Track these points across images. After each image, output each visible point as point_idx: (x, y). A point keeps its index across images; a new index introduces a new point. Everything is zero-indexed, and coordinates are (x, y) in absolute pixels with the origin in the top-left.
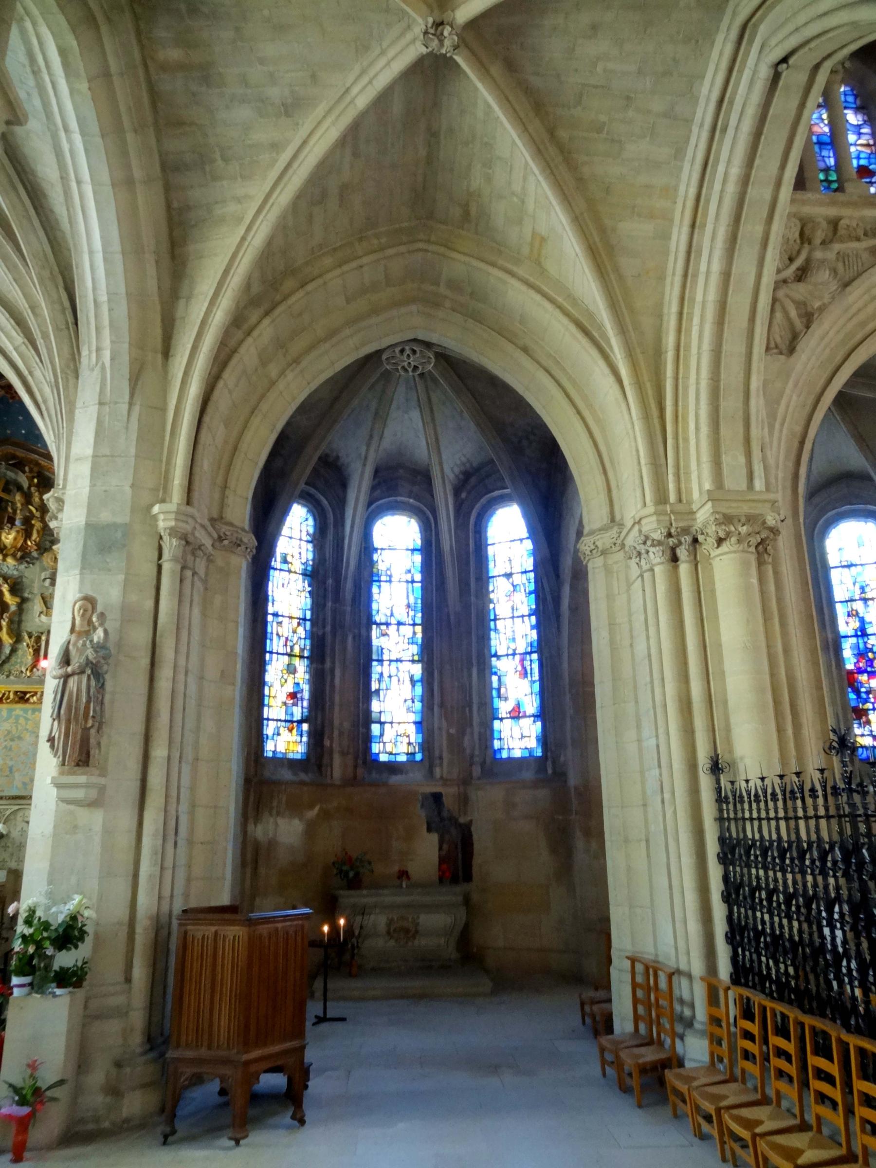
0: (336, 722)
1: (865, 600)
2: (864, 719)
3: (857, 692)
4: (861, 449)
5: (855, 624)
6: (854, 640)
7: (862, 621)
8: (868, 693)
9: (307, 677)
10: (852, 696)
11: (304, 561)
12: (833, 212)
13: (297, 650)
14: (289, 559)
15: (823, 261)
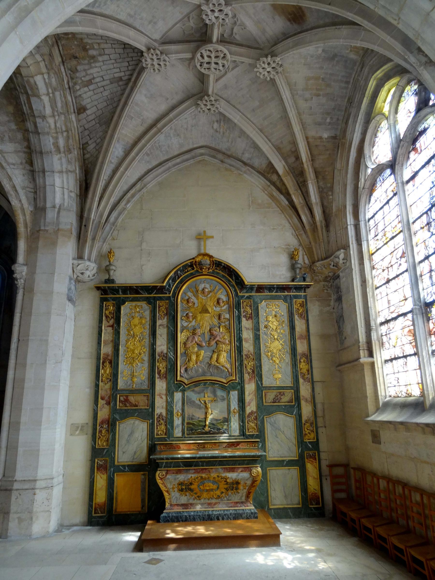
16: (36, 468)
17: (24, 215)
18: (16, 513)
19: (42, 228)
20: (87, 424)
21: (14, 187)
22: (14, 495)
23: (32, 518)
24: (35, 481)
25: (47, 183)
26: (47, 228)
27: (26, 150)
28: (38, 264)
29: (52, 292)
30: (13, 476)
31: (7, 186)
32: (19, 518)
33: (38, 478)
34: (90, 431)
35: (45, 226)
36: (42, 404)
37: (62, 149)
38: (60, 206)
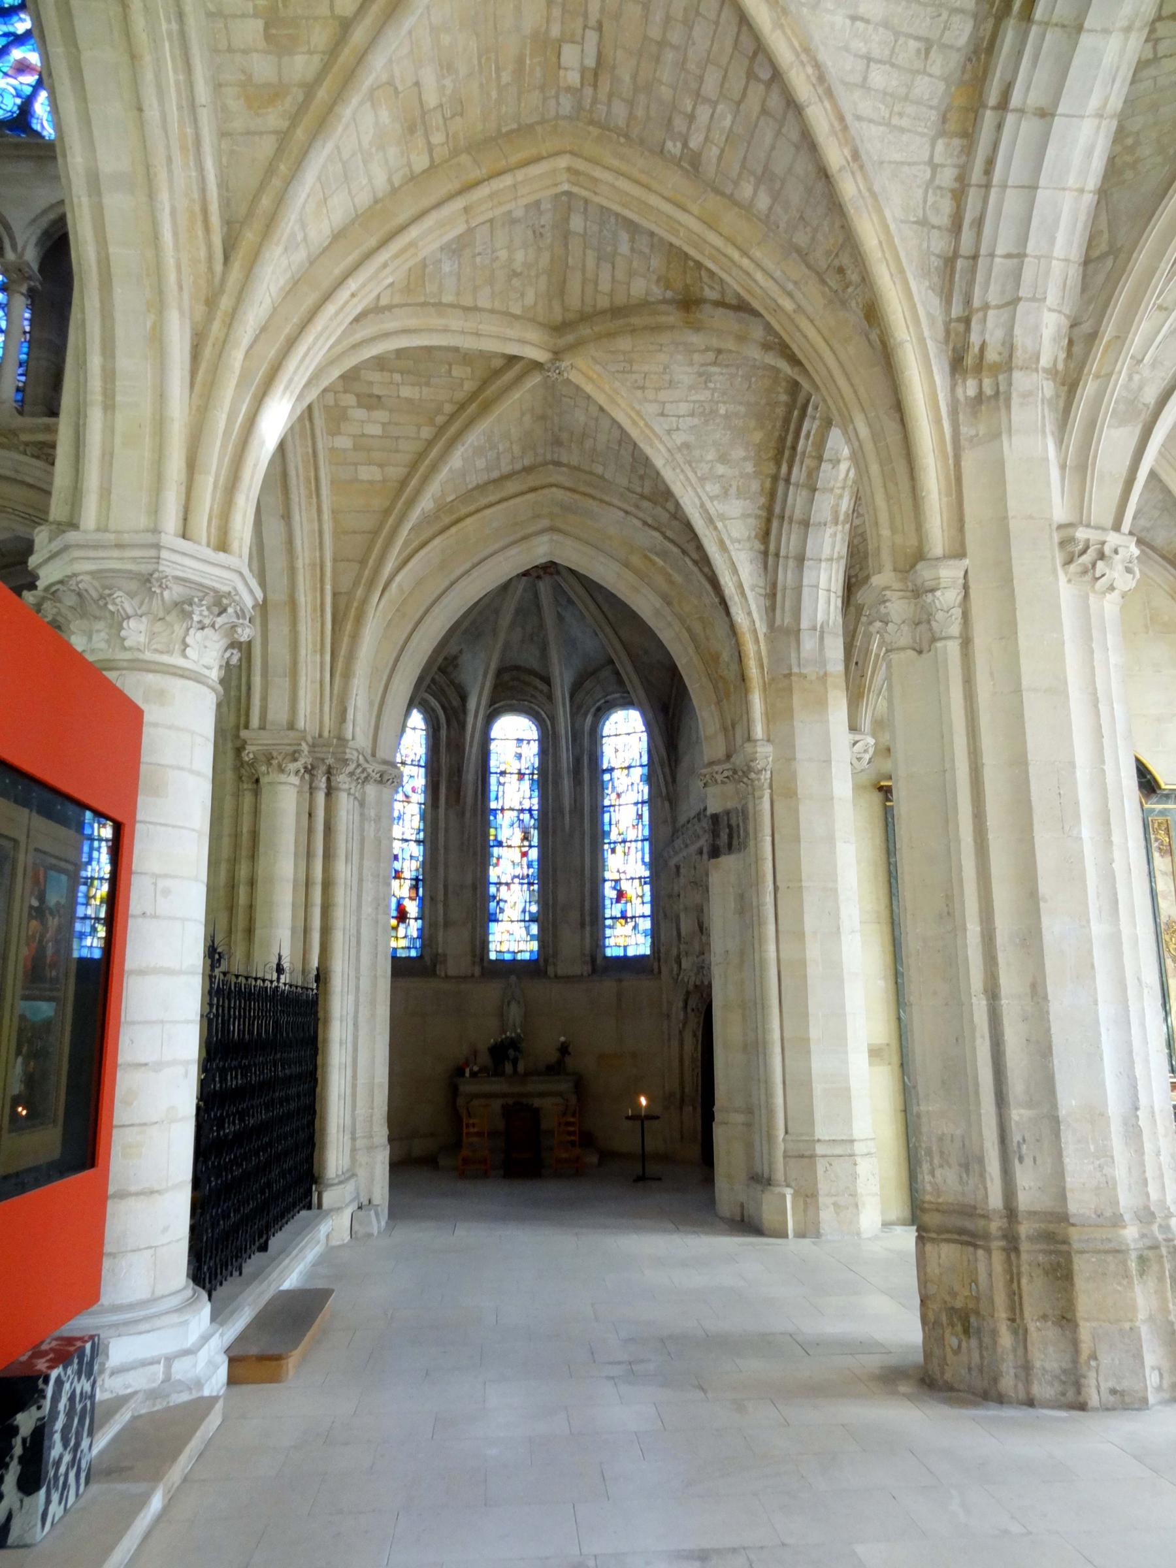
16: (848, 1120)
17: (757, 641)
18: (829, 1195)
19: (795, 670)
20: (888, 1045)
21: (740, 586)
22: (821, 1165)
23: (857, 1206)
24: (852, 1141)
25: (805, 582)
26: (804, 671)
27: (760, 512)
28: (797, 743)
29: (832, 798)
30: (813, 1134)
31: (730, 584)
32: (835, 1204)
33: (855, 1137)
34: (895, 1059)
35: (799, 665)
36: (843, 1007)
37: (842, 517)
38: (822, 627)
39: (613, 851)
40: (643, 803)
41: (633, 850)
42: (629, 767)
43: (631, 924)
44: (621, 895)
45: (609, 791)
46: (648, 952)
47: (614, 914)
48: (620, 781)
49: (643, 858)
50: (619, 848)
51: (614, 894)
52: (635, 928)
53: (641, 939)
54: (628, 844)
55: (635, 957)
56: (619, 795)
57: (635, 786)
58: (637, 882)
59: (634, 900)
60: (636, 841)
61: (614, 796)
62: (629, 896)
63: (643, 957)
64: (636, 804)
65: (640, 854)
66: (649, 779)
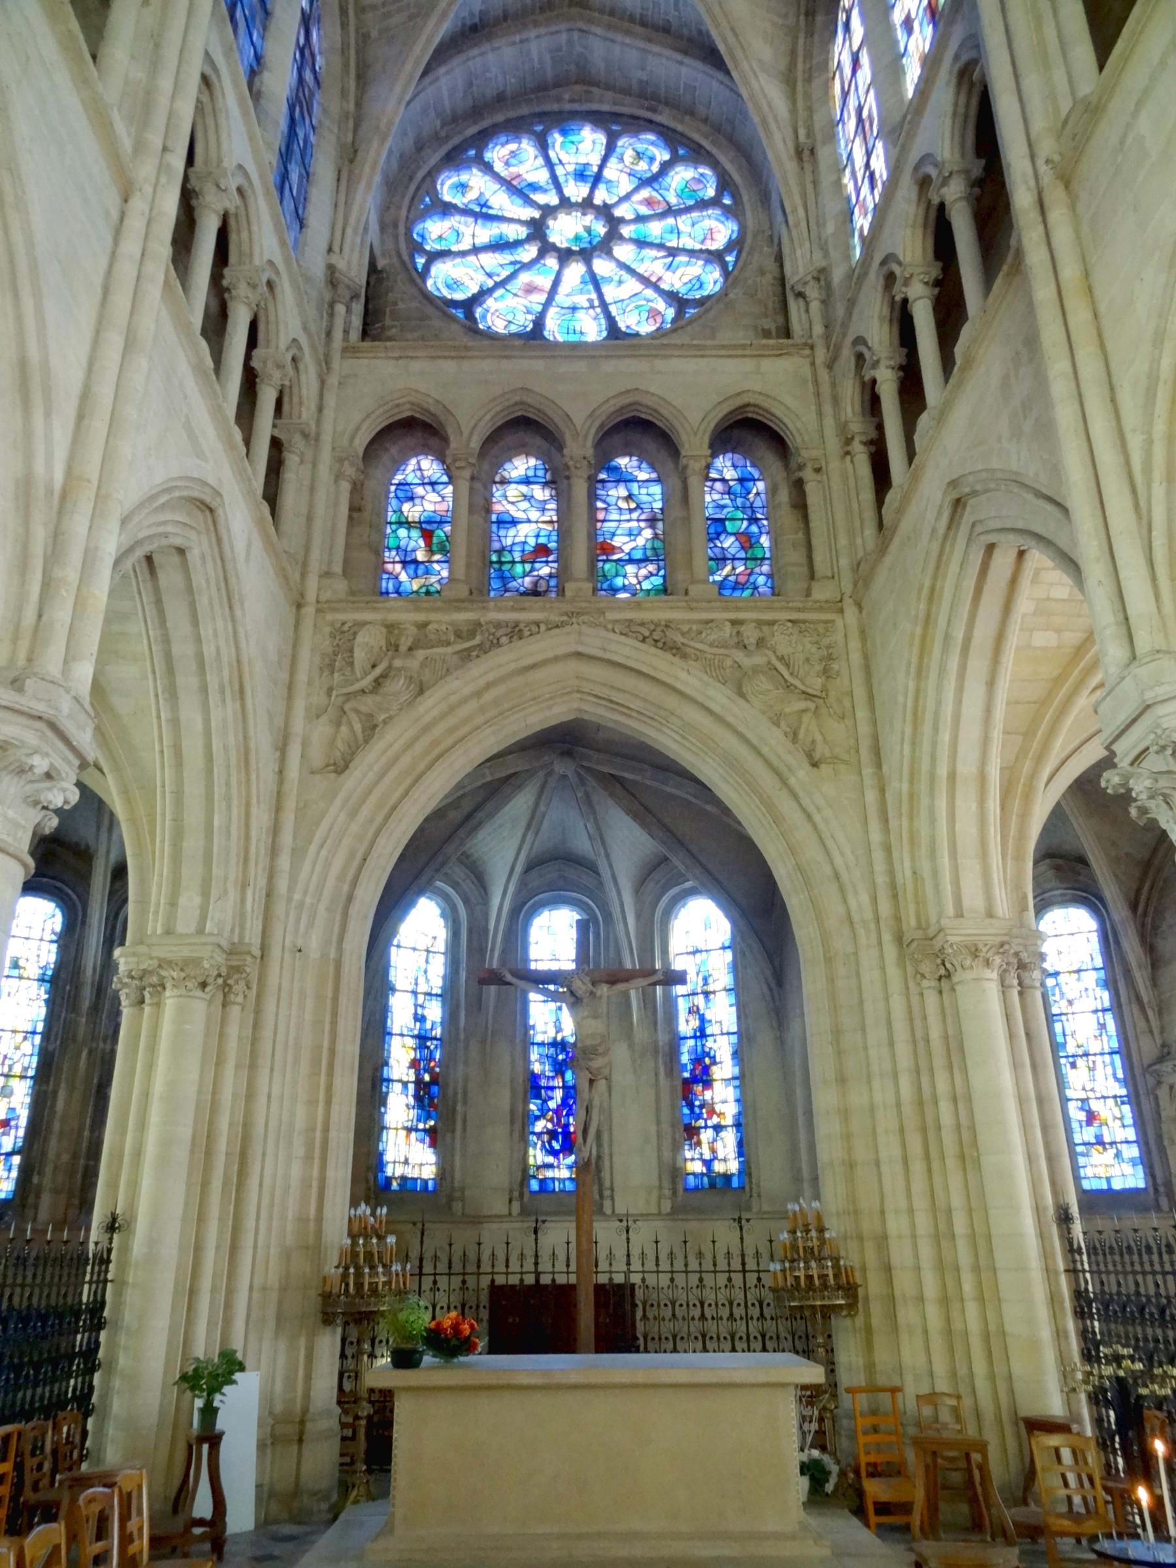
0: (51, 1155)
1: (706, 994)
2: (695, 1140)
3: (691, 1106)
4: (644, 825)
5: (695, 1023)
6: (691, 1042)
7: (702, 1019)
8: (701, 1107)
9: (28, 1100)
10: (686, 1111)
11: (42, 964)
12: (421, 617)
13: (17, 1070)
14: (21, 963)
15: (399, 670)
39: (1073, 1065)
40: (1104, 1010)
41: (1099, 1065)
42: (1078, 971)
43: (1112, 1152)
44: (1091, 1117)
45: (1057, 998)
46: (1141, 1184)
47: (1086, 1139)
48: (1070, 985)
49: (1114, 1075)
50: (1080, 1062)
51: (1082, 1116)
52: (1118, 1155)
53: (1127, 1169)
54: (1091, 1058)
55: (1124, 1191)
56: (1070, 1003)
57: (1090, 992)
58: (1111, 1102)
59: (1110, 1122)
60: (1102, 1054)
61: (1064, 1003)
62: (1103, 1117)
63: (1136, 1191)
64: (1095, 1011)
65: (1109, 1070)
66: (1109, 983)
